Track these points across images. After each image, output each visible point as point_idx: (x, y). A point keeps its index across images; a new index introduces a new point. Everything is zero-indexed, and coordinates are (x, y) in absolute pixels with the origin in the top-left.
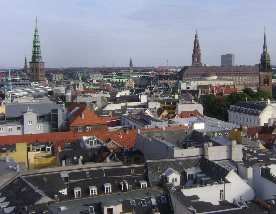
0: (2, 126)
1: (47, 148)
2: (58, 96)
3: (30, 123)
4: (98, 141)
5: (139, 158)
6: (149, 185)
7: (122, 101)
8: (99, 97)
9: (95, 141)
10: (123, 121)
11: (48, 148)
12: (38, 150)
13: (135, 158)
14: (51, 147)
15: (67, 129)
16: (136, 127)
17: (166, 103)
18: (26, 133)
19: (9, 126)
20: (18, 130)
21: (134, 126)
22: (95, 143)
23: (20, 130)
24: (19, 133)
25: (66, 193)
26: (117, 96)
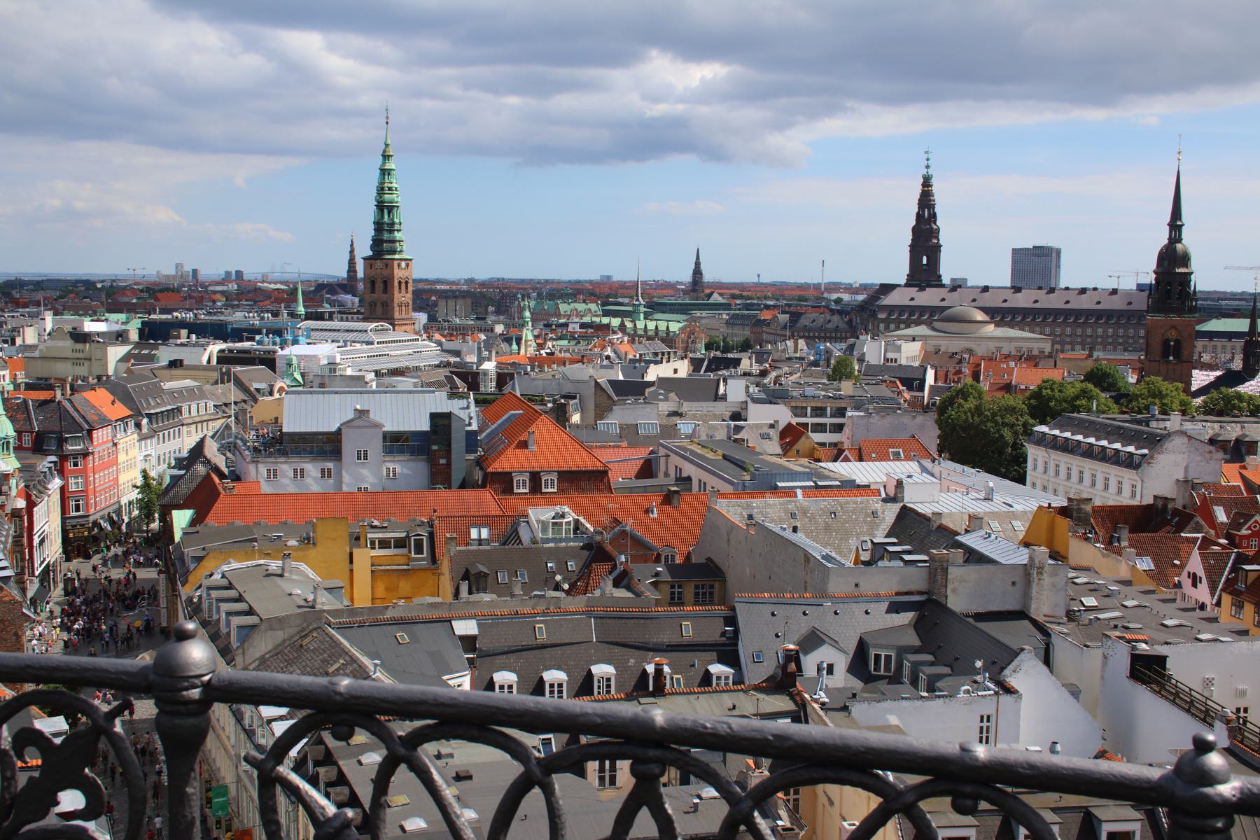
4: (577, 522)
5: (712, 587)
6: (739, 680)
7: (661, 394)
8: (587, 379)
9: (568, 523)
10: (663, 460)
12: (384, 544)
13: (697, 587)
14: (425, 538)
15: (480, 482)
16: (705, 484)
17: (809, 409)
19: (296, 464)
21: (700, 481)
22: (568, 531)
23: (329, 476)
24: (329, 485)
25: (467, 686)
26: (645, 379)
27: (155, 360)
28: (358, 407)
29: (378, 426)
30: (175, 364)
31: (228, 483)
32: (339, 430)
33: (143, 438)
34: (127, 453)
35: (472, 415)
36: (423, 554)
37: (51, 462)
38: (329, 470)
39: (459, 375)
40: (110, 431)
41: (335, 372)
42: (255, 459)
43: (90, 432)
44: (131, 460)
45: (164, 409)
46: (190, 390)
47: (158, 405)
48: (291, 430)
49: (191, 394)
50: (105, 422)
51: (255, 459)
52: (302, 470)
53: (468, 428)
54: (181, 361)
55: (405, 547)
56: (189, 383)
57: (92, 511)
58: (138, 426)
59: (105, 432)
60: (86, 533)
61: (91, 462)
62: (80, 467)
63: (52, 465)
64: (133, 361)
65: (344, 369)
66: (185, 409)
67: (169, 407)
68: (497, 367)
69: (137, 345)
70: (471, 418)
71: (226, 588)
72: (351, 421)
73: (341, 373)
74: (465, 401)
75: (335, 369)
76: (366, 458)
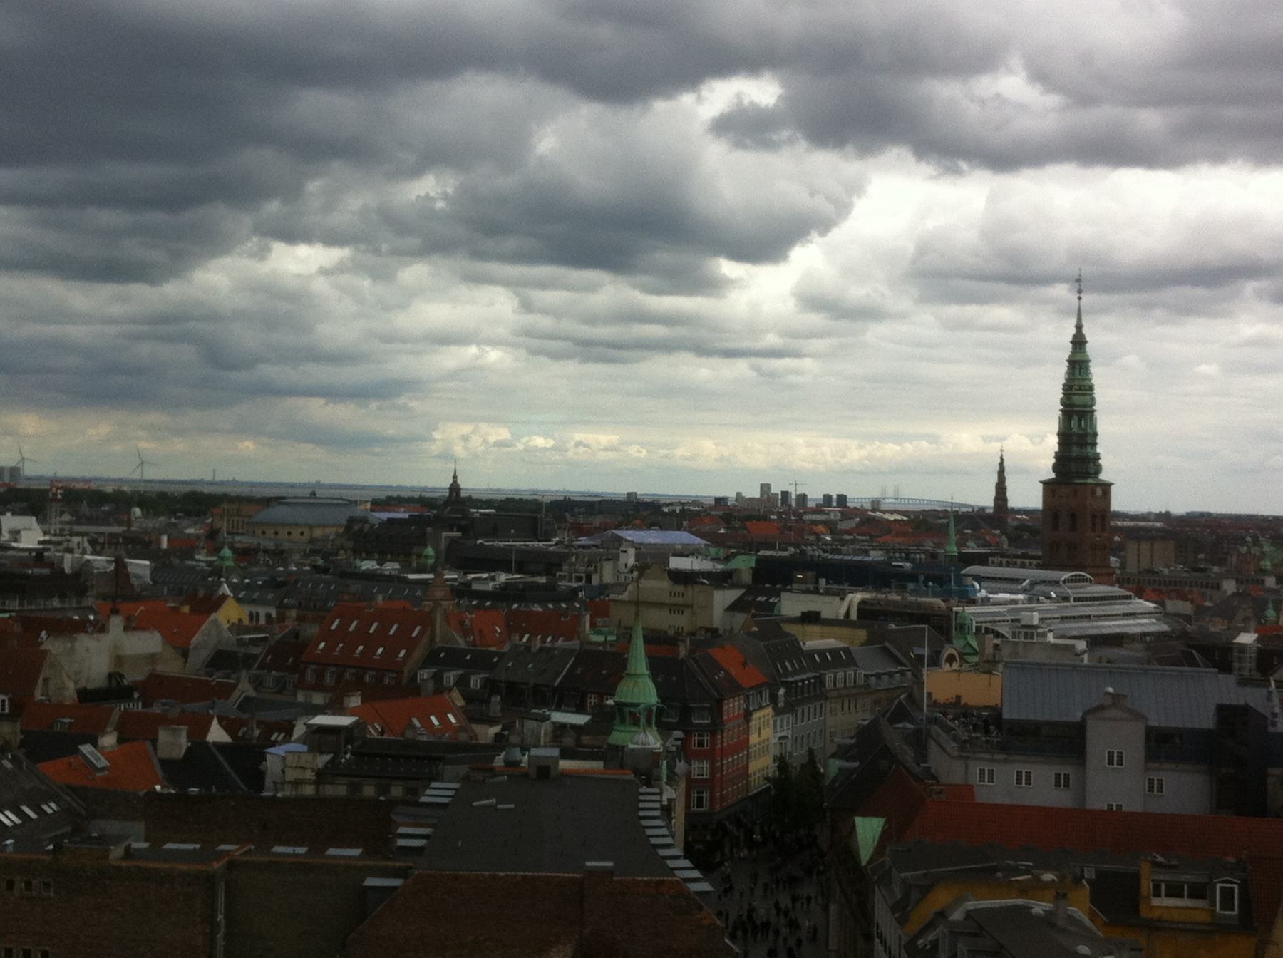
0: (988, 760)
1: (1218, 886)
2: (1189, 646)
3: (1115, 759)
11: (1221, 888)
14: (1236, 886)
18: (1097, 802)
20: (1058, 784)
23: (1067, 785)
24: (1060, 799)
27: (776, 612)
28: (1111, 690)
29: (1138, 716)
30: (811, 618)
31: (932, 785)
32: (1084, 720)
33: (778, 712)
34: (760, 734)
35: (1277, 710)
36: (1233, 910)
37: (677, 739)
38: (1067, 776)
39: (1200, 649)
40: (742, 702)
41: (1032, 638)
42: (964, 754)
43: (720, 701)
44: (764, 741)
45: (804, 677)
46: (835, 652)
47: (795, 672)
48: (1015, 717)
49: (839, 659)
50: (735, 689)
51: (964, 754)
52: (1028, 774)
53: (1271, 729)
54: (818, 614)
55: (1203, 897)
56: (831, 643)
57: (718, 807)
58: (774, 699)
59: (731, 705)
60: (708, 838)
61: (719, 742)
62: (705, 747)
63: (679, 743)
64: (753, 611)
65: (1044, 635)
66: (829, 677)
67: (810, 675)
68: (1258, 640)
69: (751, 590)
70: (1275, 715)
71: (976, 935)
72: (1101, 708)
73: (1041, 640)
74: (1264, 691)
75: (1032, 634)
76: (1120, 762)
